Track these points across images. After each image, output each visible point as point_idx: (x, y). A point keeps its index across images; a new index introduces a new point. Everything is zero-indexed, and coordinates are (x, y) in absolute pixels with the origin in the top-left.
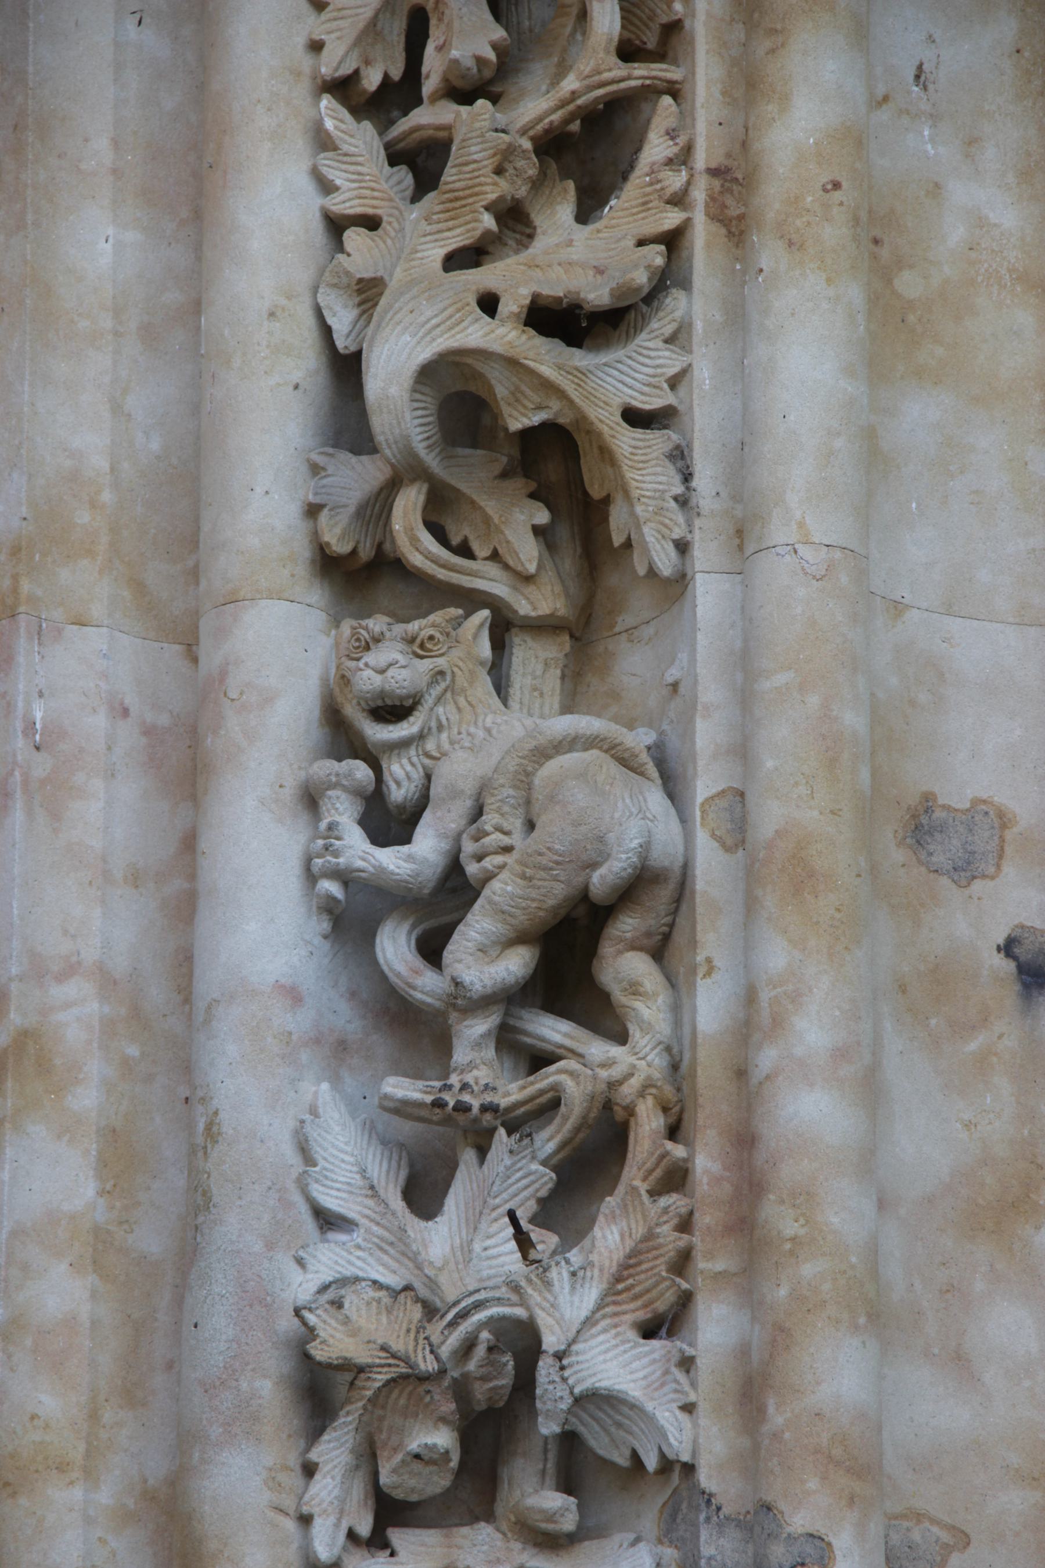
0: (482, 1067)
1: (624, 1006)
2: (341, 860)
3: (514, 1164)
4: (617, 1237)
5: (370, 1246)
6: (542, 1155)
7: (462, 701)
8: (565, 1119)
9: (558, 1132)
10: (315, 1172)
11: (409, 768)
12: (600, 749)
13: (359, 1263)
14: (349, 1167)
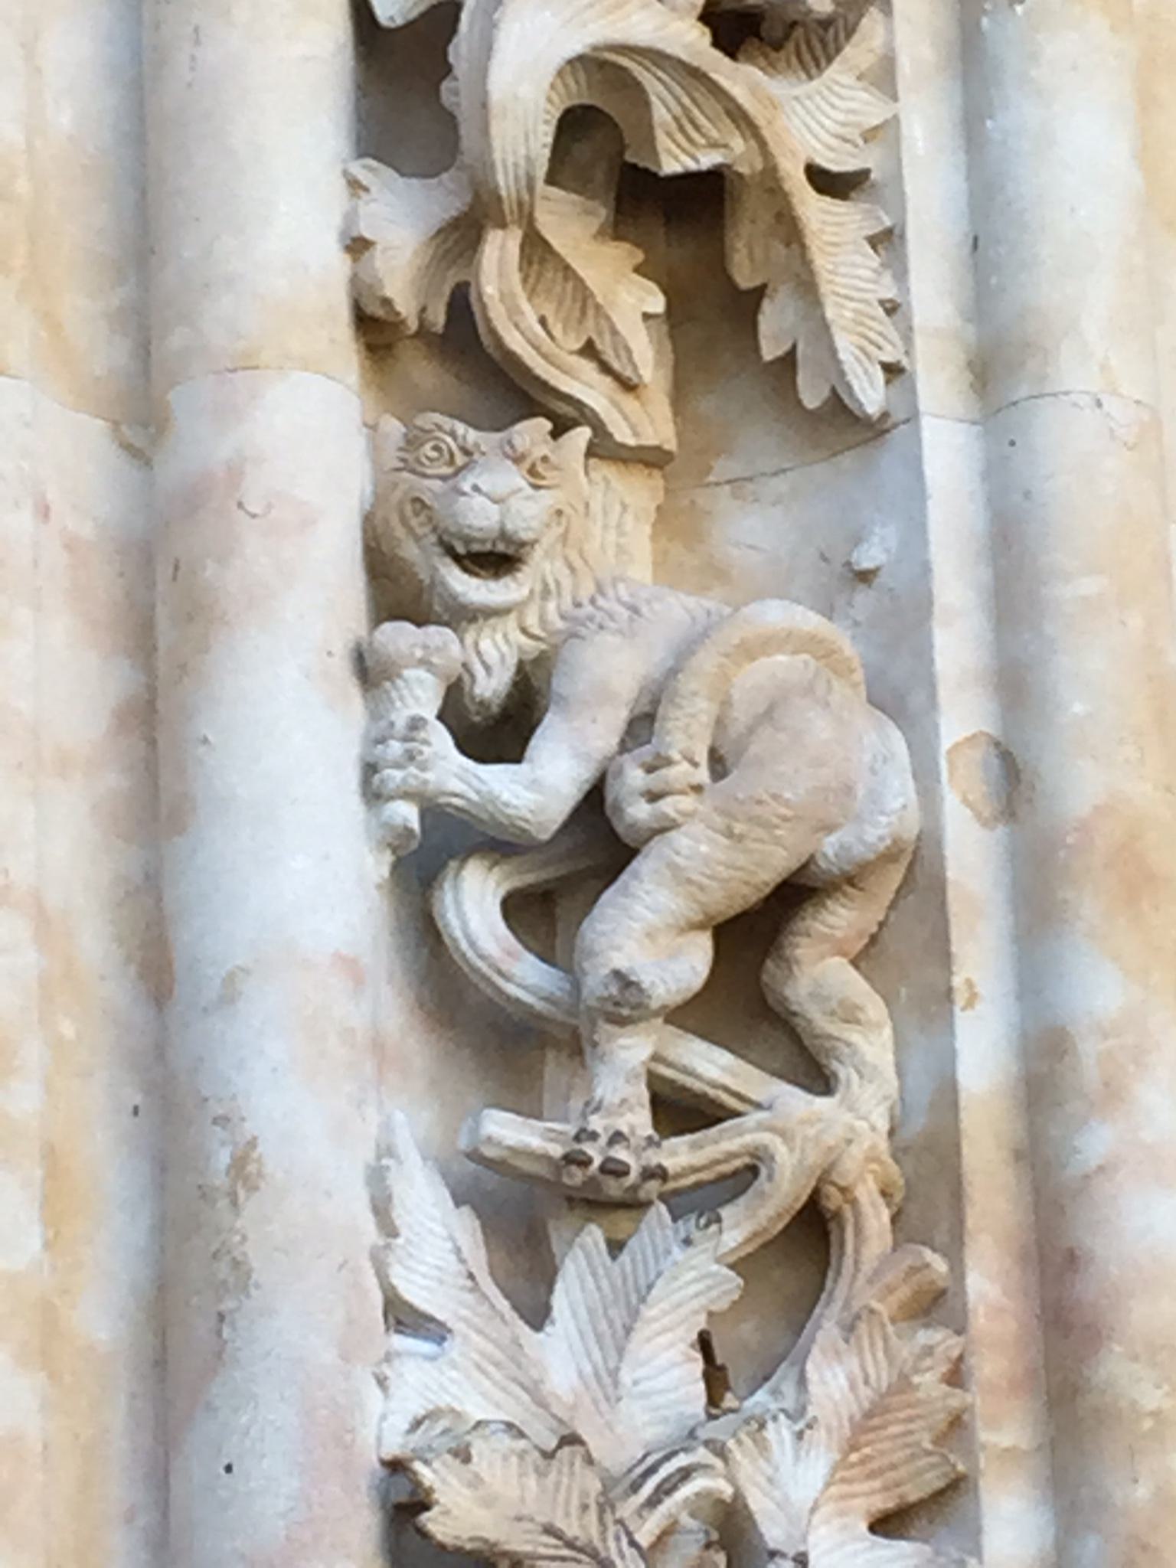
1: (830, 1037)
2: (429, 776)
4: (843, 1381)
6: (723, 1250)
11: (505, 648)
13: (453, 1389)
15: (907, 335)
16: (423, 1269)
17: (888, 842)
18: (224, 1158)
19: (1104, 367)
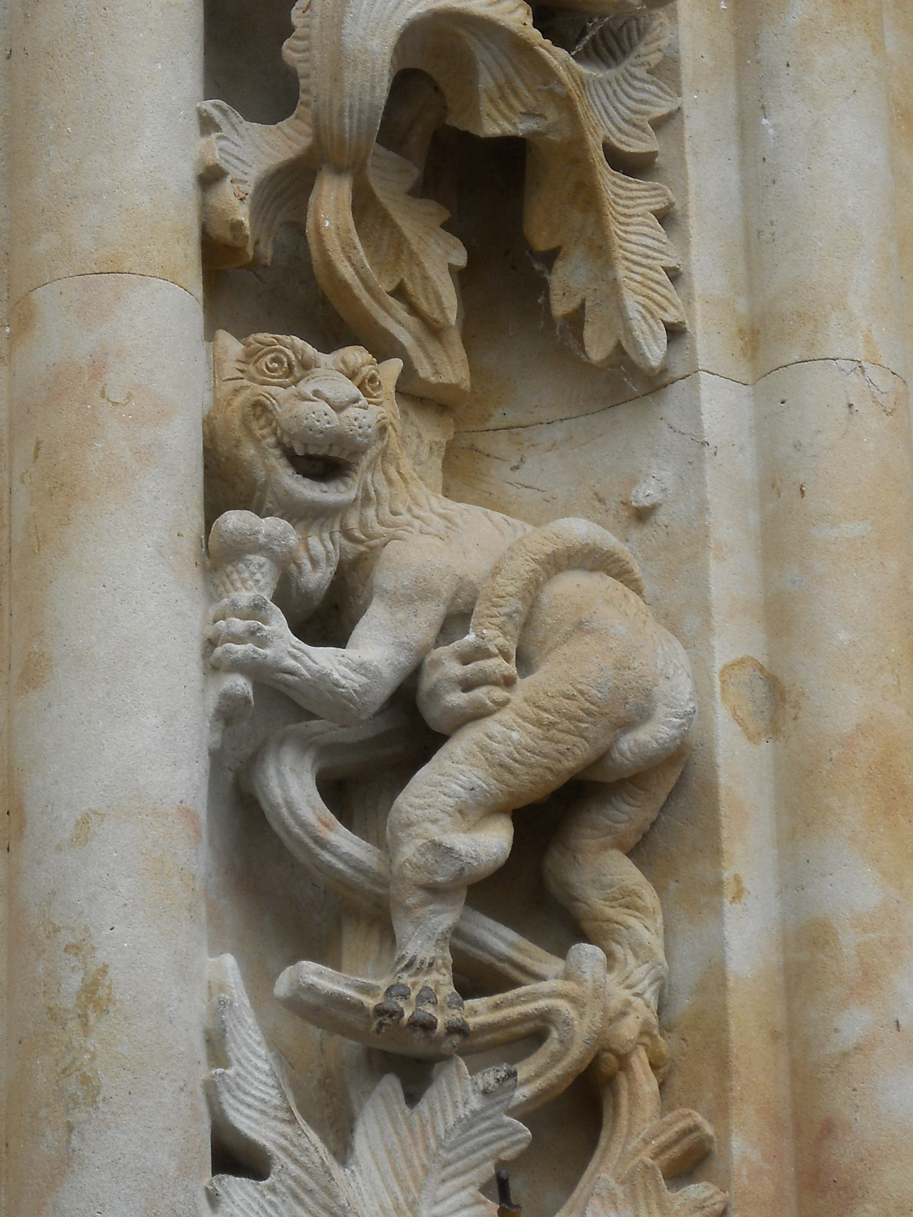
0: (444, 971)
1: (608, 920)
2: (268, 652)
3: (483, 1110)
5: (284, 1190)
6: (514, 1103)
7: (392, 471)
8: (556, 1058)
9: (537, 1076)
10: (229, 1076)
11: (330, 546)
12: (609, 573)
14: (263, 1078)
15: (689, 301)
16: (249, 1100)
17: (678, 741)
18: (75, 981)
19: (868, 340)
